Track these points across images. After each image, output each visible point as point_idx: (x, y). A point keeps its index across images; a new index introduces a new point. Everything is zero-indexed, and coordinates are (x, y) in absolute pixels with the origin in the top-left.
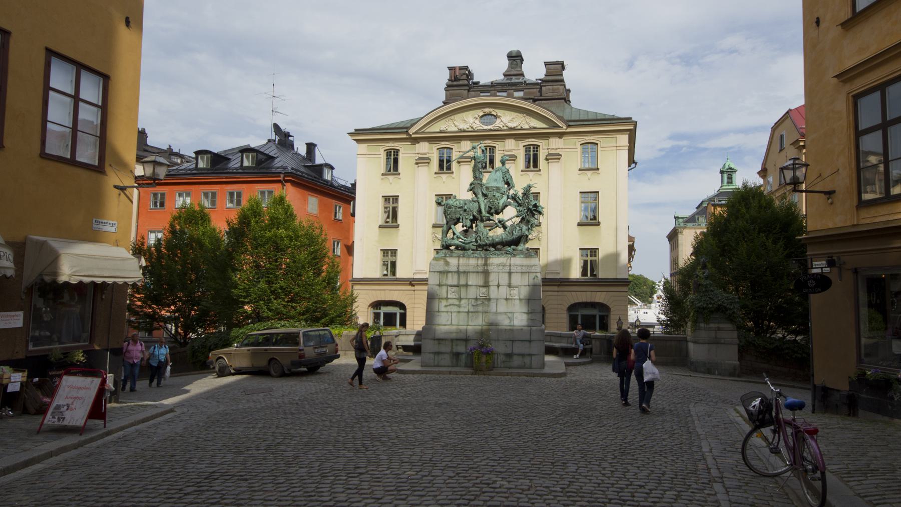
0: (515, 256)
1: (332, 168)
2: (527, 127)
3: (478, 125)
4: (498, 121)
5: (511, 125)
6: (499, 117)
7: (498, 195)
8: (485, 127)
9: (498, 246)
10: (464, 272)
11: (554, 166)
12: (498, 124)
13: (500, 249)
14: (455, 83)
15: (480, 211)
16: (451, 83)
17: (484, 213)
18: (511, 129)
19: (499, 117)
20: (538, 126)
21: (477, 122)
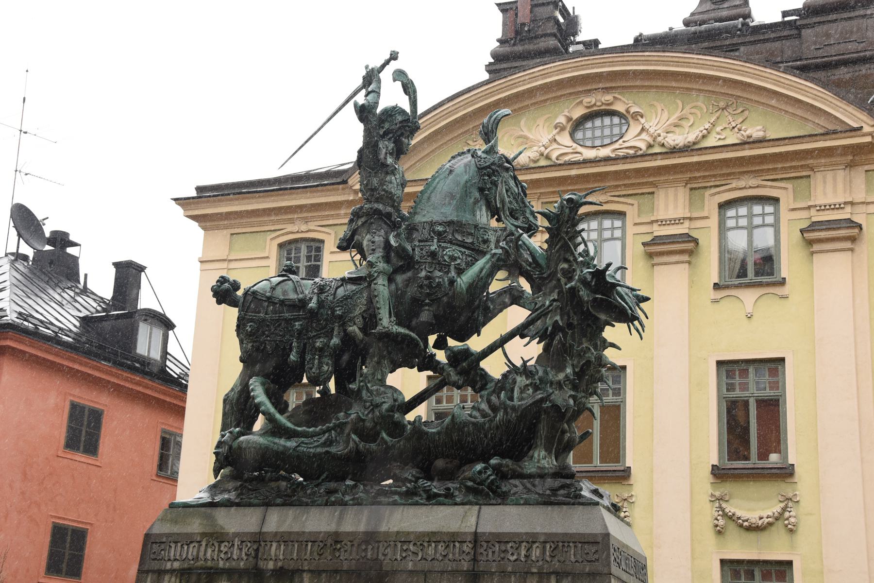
0: (503, 498)
1: (167, 325)
2: (732, 139)
3: (565, 147)
4: (635, 129)
5: (677, 139)
6: (637, 116)
7: (451, 251)
8: (590, 154)
9: (444, 461)
10: (280, 572)
11: (834, 270)
12: (634, 139)
13: (446, 475)
14: (519, 48)
15: (371, 319)
16: (507, 49)
17: (386, 322)
18: (674, 151)
19: (637, 116)
20: (772, 135)
21: (565, 139)
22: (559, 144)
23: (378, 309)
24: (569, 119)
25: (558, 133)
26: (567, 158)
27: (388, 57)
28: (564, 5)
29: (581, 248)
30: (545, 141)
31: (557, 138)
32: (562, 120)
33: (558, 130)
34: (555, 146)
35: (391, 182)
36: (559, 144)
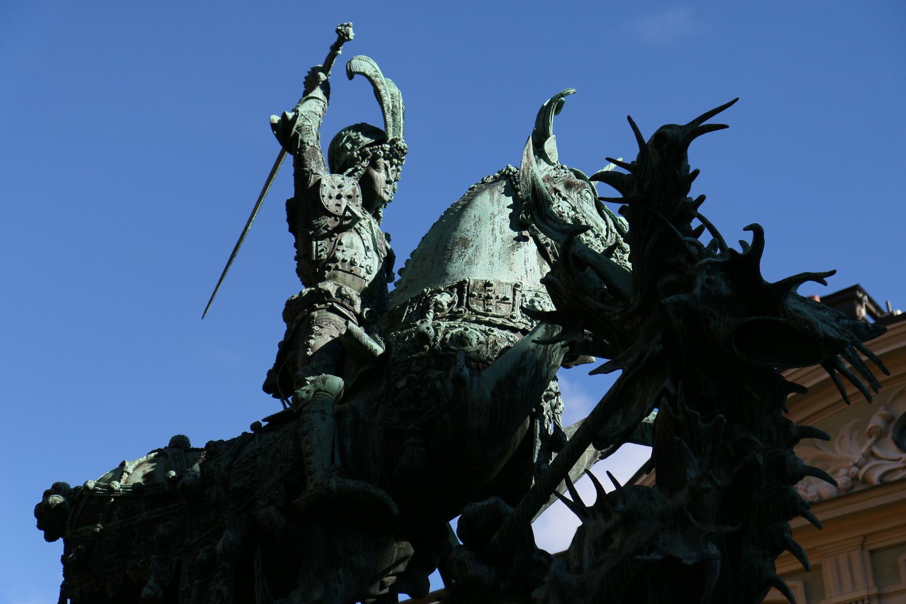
21: (889, 450)
22: (878, 458)
23: (309, 454)
24: (889, 420)
25: (876, 442)
26: (896, 477)
27: (335, 38)
28: (871, 300)
29: (705, 239)
30: (857, 457)
31: (876, 450)
32: (877, 421)
33: (872, 439)
34: (874, 462)
35: (351, 246)
36: (878, 458)
